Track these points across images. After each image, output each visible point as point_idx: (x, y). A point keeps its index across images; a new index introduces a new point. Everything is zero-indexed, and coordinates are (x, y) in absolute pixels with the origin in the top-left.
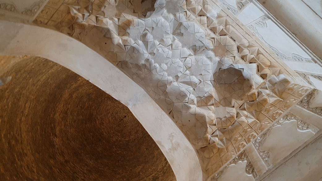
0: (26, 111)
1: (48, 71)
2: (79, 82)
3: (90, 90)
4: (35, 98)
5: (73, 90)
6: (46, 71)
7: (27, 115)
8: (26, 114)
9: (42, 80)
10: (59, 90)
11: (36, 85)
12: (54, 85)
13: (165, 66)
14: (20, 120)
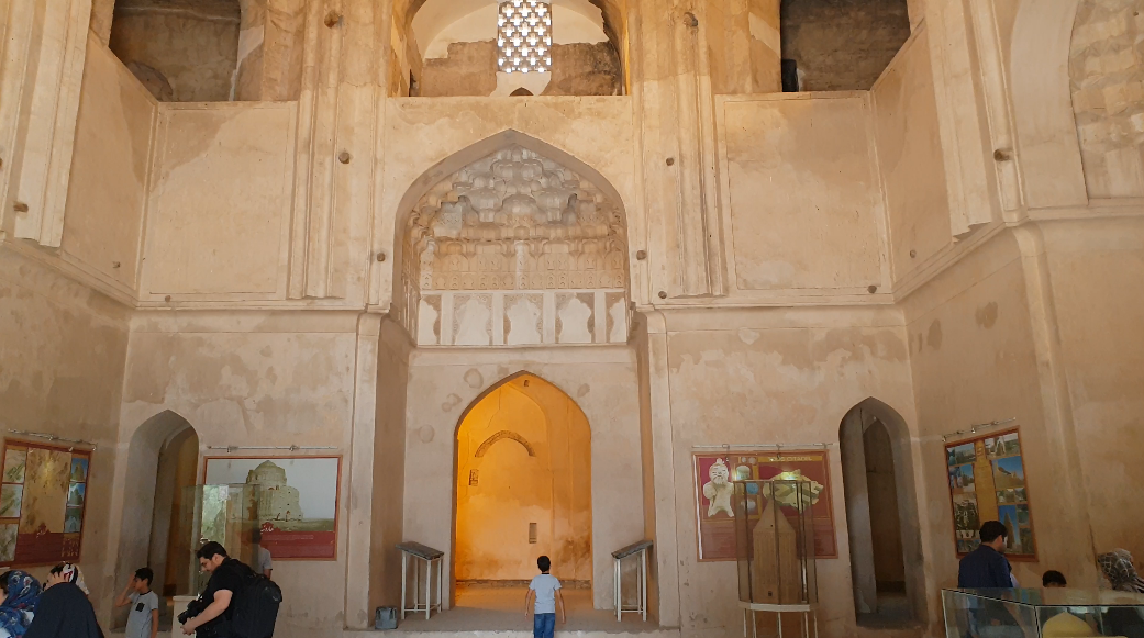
13: (516, 158)
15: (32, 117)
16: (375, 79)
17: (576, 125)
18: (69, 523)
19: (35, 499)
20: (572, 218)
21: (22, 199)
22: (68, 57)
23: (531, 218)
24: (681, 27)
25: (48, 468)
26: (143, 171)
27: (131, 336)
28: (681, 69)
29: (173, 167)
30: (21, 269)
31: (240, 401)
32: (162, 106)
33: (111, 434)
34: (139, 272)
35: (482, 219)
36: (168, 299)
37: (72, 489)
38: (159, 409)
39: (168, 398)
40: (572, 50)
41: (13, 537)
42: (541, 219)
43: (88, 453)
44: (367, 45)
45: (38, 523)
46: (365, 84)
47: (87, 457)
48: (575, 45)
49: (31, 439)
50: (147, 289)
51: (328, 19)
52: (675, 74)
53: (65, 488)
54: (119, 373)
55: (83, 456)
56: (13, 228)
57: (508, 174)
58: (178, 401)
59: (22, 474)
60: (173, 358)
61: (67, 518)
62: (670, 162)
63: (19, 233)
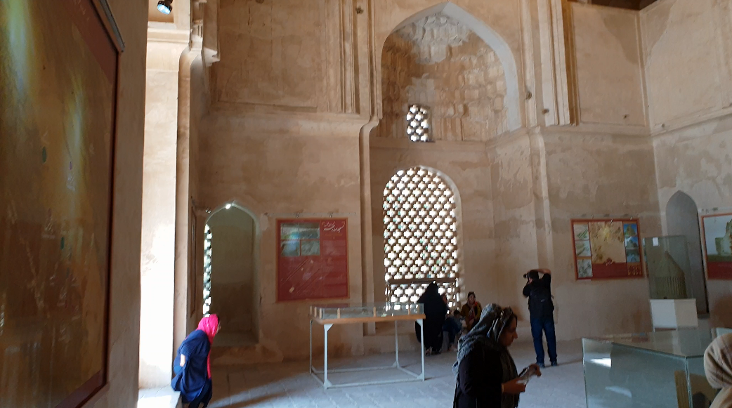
15: (542, 66)
18: (630, 258)
19: (600, 247)
21: (545, 107)
22: (555, 25)
25: (605, 231)
26: (635, 55)
27: (655, 150)
29: (652, 47)
30: (559, 138)
31: (713, 179)
32: (642, 13)
33: (656, 207)
34: (647, 115)
36: (663, 126)
37: (627, 240)
38: (674, 191)
39: (678, 182)
41: (589, 266)
43: (636, 220)
45: (605, 259)
47: (635, 223)
49: (589, 217)
50: (654, 127)
53: (621, 239)
54: (652, 172)
55: (632, 224)
56: (544, 122)
58: (682, 184)
59: (587, 234)
60: (676, 159)
61: (627, 255)
63: (548, 124)
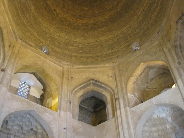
0: (142, 9)
1: (120, 33)
2: (109, 15)
3: (106, 4)
4: (134, 15)
5: (115, 8)
6: (121, 35)
7: (143, 6)
8: (143, 7)
9: (126, 28)
10: (122, 13)
11: (130, 26)
12: (123, 19)
14: (146, 6)
16: (7, 87)
17: (47, 114)
20: (27, 134)
23: (18, 131)
24: (69, 103)
28: (68, 111)
35: (8, 127)
40: (33, 97)
42: (21, 131)
44: (8, 78)
46: (5, 87)
48: (33, 96)
51: (3, 69)
52: (67, 111)
57: (20, 119)
62: (65, 129)
